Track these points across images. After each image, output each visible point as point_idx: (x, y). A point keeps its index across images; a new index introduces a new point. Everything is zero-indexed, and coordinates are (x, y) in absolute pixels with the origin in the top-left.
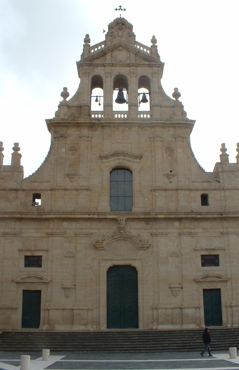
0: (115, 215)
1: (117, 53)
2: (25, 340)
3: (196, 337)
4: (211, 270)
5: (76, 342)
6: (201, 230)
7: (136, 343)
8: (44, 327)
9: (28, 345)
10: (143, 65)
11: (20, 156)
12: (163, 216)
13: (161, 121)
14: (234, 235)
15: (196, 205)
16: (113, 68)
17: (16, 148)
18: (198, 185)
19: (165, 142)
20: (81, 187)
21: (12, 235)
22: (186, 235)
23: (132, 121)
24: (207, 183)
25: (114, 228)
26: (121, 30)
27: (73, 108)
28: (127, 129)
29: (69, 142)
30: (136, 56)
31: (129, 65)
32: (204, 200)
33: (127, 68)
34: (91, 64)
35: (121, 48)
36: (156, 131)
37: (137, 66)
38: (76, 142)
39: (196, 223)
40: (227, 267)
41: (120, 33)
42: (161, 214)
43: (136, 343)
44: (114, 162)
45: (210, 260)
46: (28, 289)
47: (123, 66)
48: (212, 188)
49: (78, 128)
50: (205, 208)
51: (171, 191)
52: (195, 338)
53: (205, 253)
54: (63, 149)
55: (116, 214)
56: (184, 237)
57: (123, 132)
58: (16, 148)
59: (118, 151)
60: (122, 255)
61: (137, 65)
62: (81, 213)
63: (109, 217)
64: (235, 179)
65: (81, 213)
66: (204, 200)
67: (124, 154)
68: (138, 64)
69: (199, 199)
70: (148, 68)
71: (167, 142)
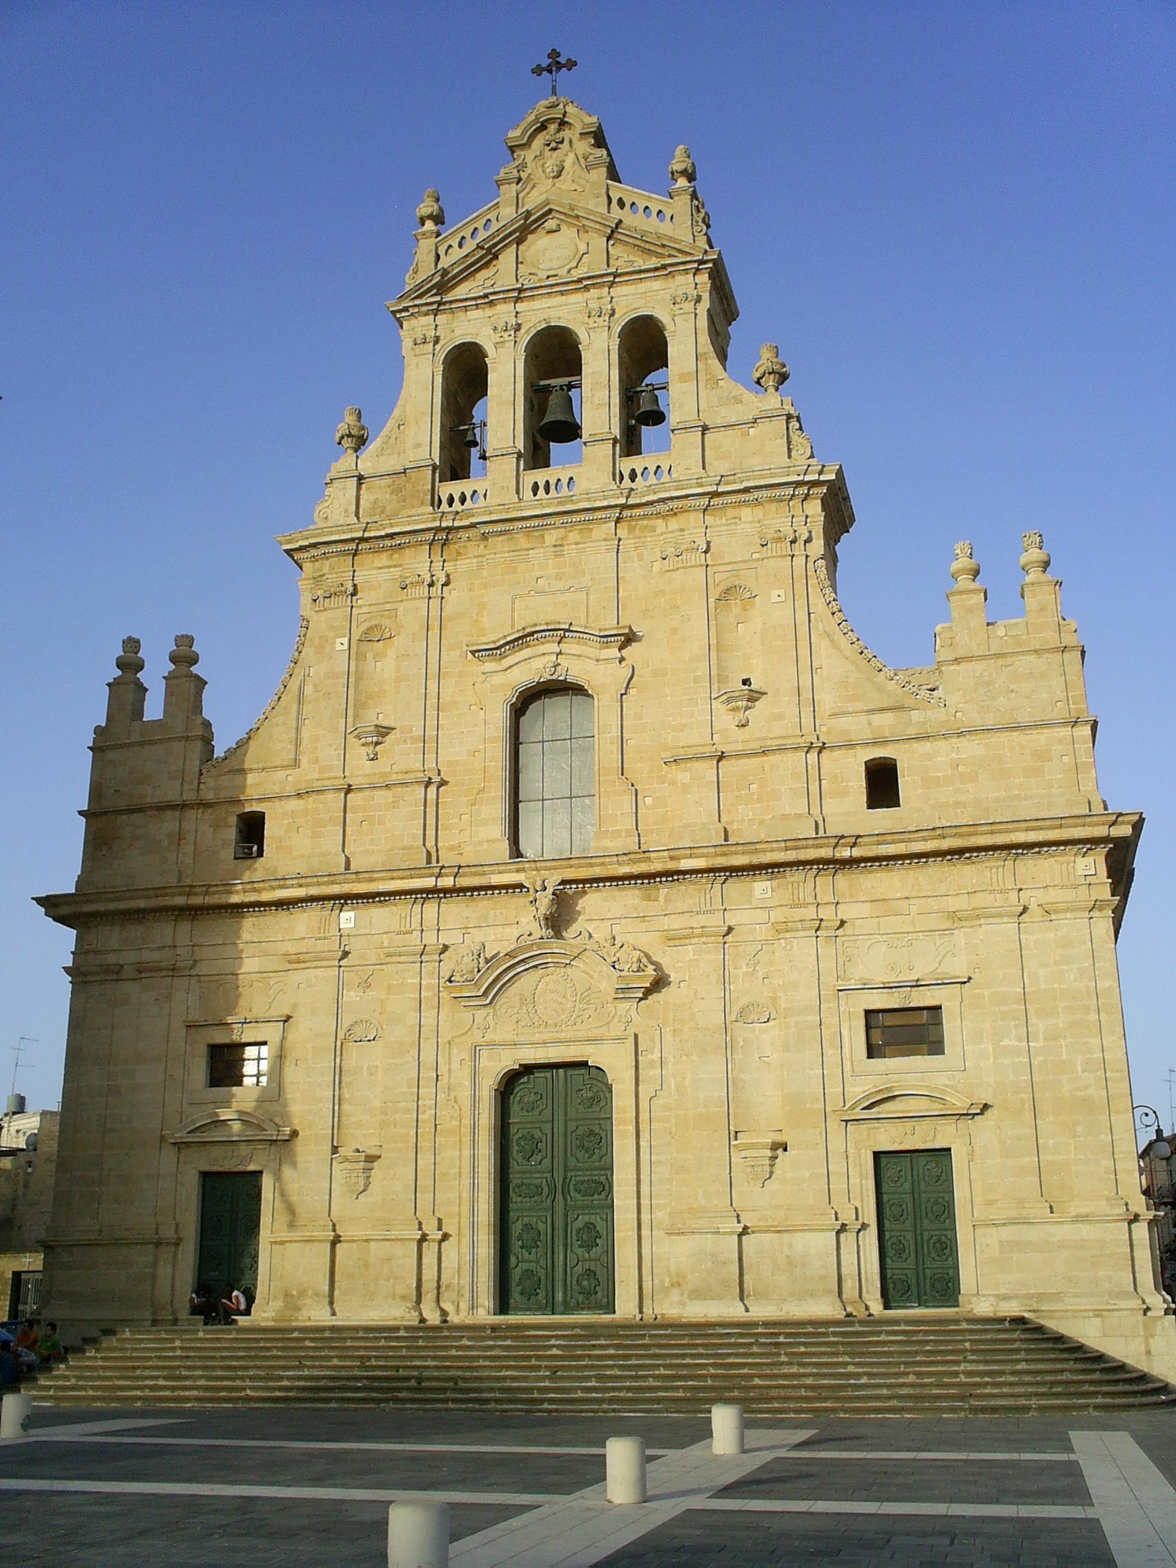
0: (518, 871)
1: (538, 244)
2: (151, 1358)
3: (786, 1354)
4: (905, 1070)
5: (242, 1378)
6: (865, 909)
7: (195, 1393)
8: (265, 1313)
9: (147, 1378)
10: (639, 274)
11: (201, 683)
12: (700, 863)
13: (701, 485)
14: (1005, 919)
15: (848, 808)
16: (520, 307)
17: (184, 657)
18: (857, 727)
19: (722, 568)
20: (405, 776)
21: (164, 973)
22: (802, 933)
23: (589, 500)
24: (889, 715)
25: (523, 920)
26: (554, 149)
27: (377, 482)
28: (573, 536)
29: (366, 609)
30: (611, 242)
31: (583, 284)
32: (882, 784)
33: (578, 298)
34: (440, 303)
35: (551, 224)
36: (682, 530)
37: (613, 282)
38: (388, 606)
39: (843, 880)
40: (973, 1056)
41: (551, 161)
42: (692, 851)
43: (195, 1393)
44: (531, 667)
45: (904, 1030)
46: (215, 1168)
47: (562, 293)
48: (912, 731)
49: (396, 556)
50: (883, 818)
51: (743, 761)
52: (784, 1359)
53: (880, 1001)
54: (341, 640)
55: (521, 866)
56: (795, 941)
57: (559, 549)
58: (184, 657)
59: (535, 625)
60: (537, 1026)
61: (614, 279)
62: (392, 873)
63: (496, 880)
64: (1012, 687)
65: (392, 873)
66: (882, 784)
67: (563, 633)
68: (616, 275)
69: (859, 783)
70: (656, 285)
71: (729, 568)
